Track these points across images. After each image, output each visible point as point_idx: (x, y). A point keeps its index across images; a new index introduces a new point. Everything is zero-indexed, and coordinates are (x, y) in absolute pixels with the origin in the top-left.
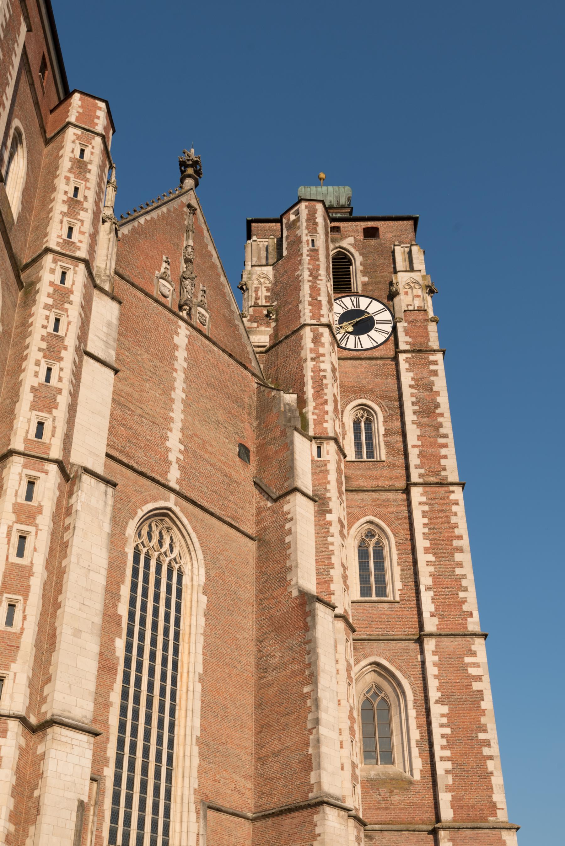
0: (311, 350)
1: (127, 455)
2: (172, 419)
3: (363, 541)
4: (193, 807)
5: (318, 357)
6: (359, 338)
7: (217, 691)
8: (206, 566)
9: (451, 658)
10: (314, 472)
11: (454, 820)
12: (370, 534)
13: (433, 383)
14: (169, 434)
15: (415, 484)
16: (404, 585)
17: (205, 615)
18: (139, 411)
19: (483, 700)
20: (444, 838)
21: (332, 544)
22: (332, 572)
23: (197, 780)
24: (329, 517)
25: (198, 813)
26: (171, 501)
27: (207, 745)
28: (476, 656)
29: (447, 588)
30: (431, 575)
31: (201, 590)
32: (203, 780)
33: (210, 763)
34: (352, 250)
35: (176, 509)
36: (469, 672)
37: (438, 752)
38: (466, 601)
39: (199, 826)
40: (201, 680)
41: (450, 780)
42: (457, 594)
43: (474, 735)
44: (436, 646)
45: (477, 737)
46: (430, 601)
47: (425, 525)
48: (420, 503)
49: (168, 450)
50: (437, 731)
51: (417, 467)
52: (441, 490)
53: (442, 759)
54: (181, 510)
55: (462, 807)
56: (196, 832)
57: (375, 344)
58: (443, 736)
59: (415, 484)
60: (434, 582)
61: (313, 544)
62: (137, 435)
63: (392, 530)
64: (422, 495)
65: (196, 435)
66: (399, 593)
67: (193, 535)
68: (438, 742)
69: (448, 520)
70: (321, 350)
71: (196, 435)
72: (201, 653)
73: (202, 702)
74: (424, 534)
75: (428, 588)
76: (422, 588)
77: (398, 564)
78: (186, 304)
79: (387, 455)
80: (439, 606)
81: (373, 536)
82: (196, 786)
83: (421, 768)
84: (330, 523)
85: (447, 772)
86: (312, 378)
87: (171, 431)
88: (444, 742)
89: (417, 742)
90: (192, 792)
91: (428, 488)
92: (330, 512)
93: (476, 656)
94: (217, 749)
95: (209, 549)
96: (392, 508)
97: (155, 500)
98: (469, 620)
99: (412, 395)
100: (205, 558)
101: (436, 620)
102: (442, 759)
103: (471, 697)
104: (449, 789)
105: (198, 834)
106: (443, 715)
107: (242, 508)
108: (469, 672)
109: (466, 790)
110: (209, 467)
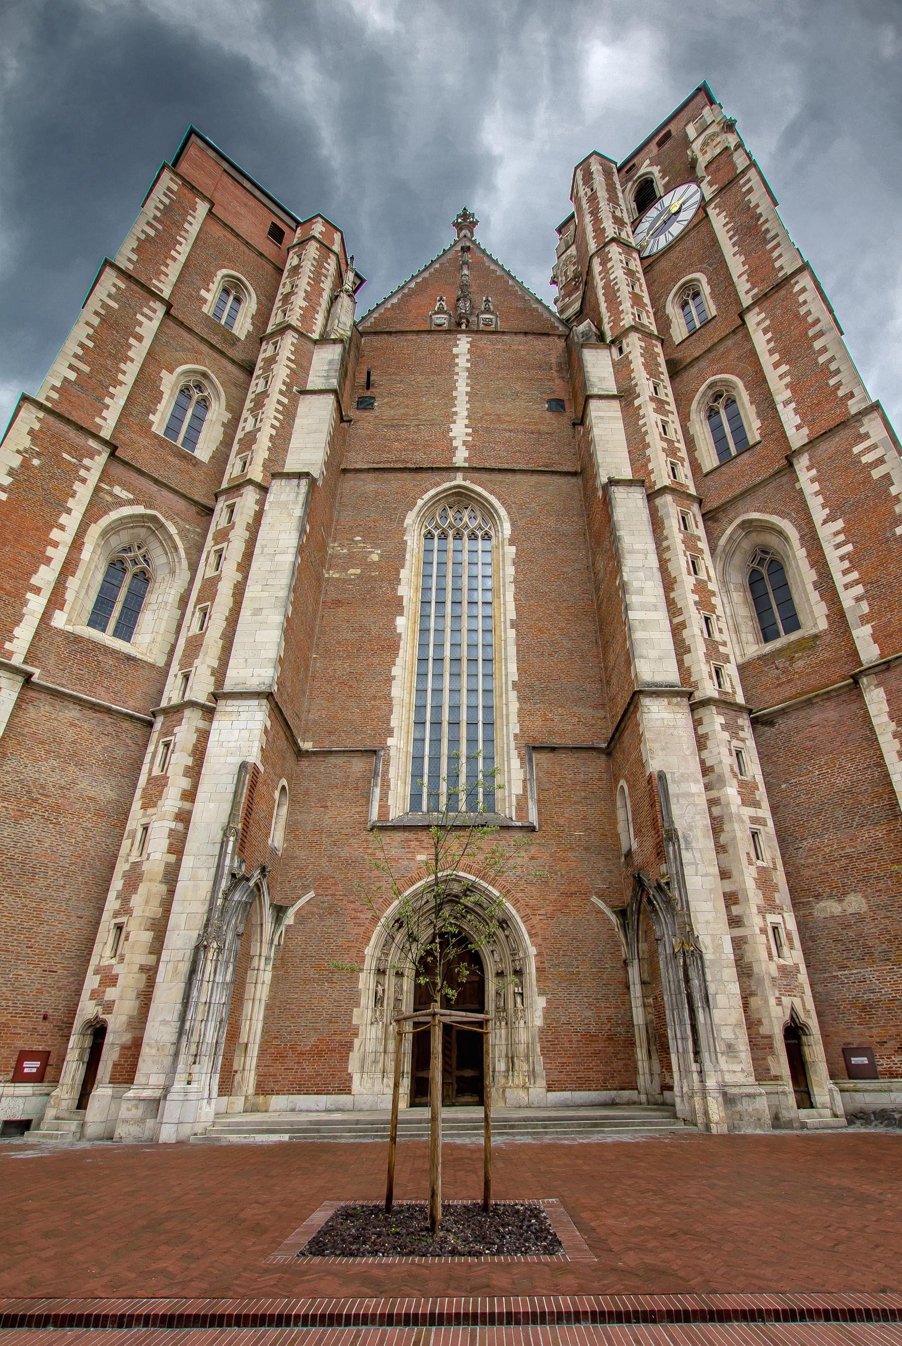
0: (600, 273)
1: (404, 461)
2: (455, 413)
3: (711, 409)
4: (514, 753)
5: (606, 272)
6: (669, 232)
7: (539, 630)
8: (511, 519)
9: (833, 461)
10: (616, 373)
11: (882, 656)
12: (717, 396)
13: (749, 201)
14: (452, 426)
15: (749, 309)
16: (763, 420)
17: (514, 564)
18: (415, 423)
19: (892, 484)
20: (869, 685)
21: (645, 425)
22: (648, 452)
23: (518, 725)
24: (637, 403)
25: (522, 759)
26: (459, 480)
27: (530, 687)
28: (869, 437)
29: (812, 386)
30: (787, 386)
31: (506, 542)
32: (527, 723)
33: (535, 704)
34: (649, 169)
35: (467, 484)
36: (864, 462)
37: (839, 580)
38: (841, 385)
39: (525, 772)
40: (514, 624)
41: (865, 607)
42: (827, 384)
43: (888, 535)
44: (810, 460)
45: (895, 534)
46: (792, 414)
47: (769, 341)
48: (758, 324)
49: (451, 439)
50: (832, 556)
51: (747, 293)
52: (783, 293)
53: (847, 587)
54: (472, 482)
55: (891, 636)
56: (522, 777)
57: (685, 223)
58: (842, 558)
59: (749, 309)
60: (794, 391)
61: (623, 437)
62: (413, 443)
63: (737, 376)
64: (758, 314)
65: (487, 414)
66: (759, 431)
67: (492, 499)
68: (836, 567)
69: (797, 315)
70: (609, 265)
71: (487, 414)
72: (512, 599)
73: (518, 645)
74: (770, 351)
75: (786, 403)
76: (780, 407)
77: (751, 403)
78: (461, 318)
79: (718, 308)
80: (805, 413)
81: (721, 396)
82: (517, 731)
83: (827, 612)
84: (639, 407)
85: (858, 599)
86: (604, 294)
87: (455, 422)
88: (846, 564)
89: (814, 583)
90: (512, 738)
91: (766, 304)
92: (638, 396)
93: (869, 437)
94: (546, 687)
95: (515, 503)
96: (734, 354)
97: (438, 484)
98: (849, 403)
99: (728, 232)
100: (509, 513)
101: (805, 431)
102: (847, 587)
103: (874, 490)
104: (864, 620)
105: (524, 781)
106: (837, 534)
107: (558, 453)
108: (864, 462)
109: (893, 611)
110: (507, 435)
